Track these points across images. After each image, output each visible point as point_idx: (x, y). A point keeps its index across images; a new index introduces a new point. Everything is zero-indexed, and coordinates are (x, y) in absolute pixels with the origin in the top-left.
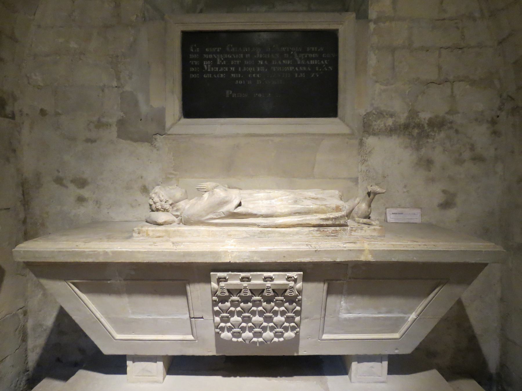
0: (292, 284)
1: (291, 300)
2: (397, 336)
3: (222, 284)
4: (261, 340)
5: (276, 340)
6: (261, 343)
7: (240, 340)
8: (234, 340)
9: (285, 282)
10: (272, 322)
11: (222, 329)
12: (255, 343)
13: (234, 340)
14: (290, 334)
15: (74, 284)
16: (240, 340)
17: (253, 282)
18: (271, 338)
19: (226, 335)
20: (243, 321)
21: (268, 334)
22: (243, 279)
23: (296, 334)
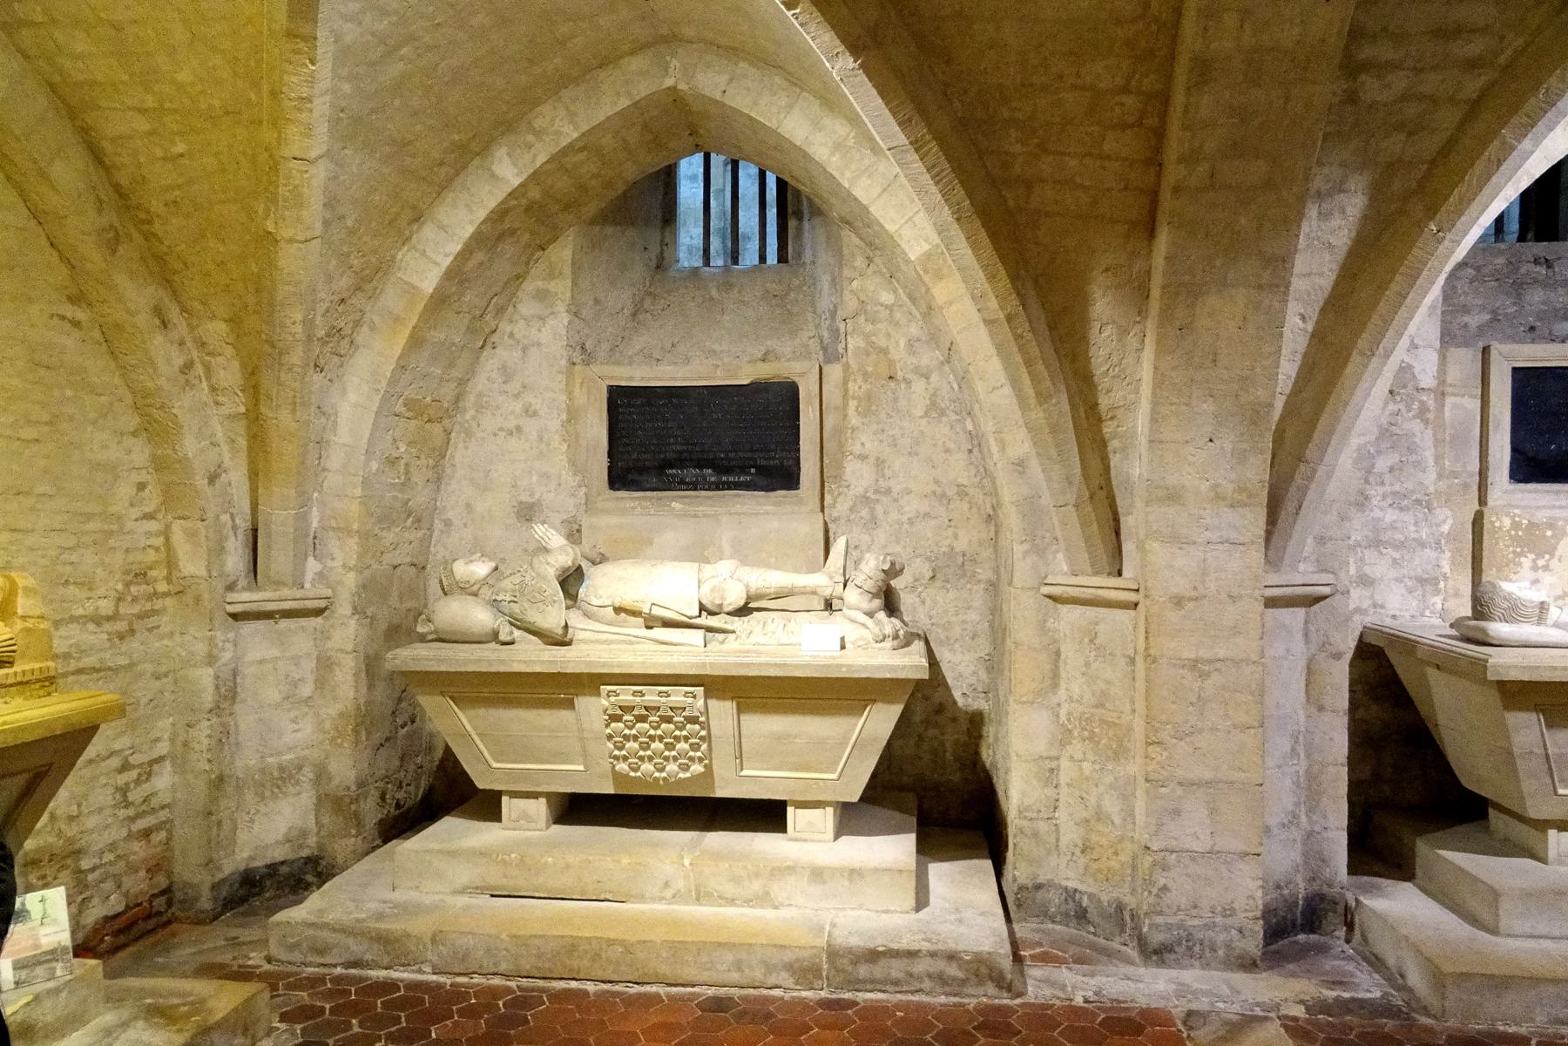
0: (690, 700)
1: (693, 720)
2: (834, 776)
3: (612, 699)
4: (664, 774)
5: (681, 775)
6: (664, 779)
7: (639, 774)
8: (632, 774)
9: (683, 699)
10: (673, 749)
11: (616, 758)
12: (656, 779)
13: (632, 774)
14: (697, 768)
15: (452, 698)
16: (639, 774)
17: (646, 698)
18: (674, 773)
19: (622, 767)
20: (642, 748)
21: (672, 767)
22: (635, 693)
23: (705, 766)
